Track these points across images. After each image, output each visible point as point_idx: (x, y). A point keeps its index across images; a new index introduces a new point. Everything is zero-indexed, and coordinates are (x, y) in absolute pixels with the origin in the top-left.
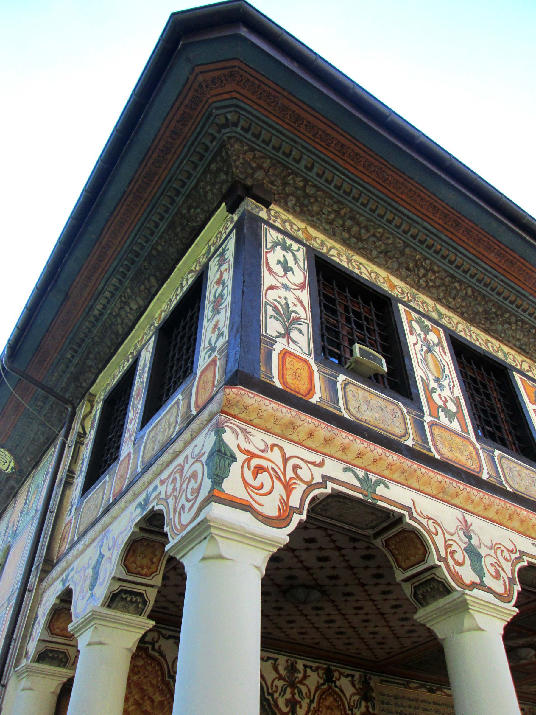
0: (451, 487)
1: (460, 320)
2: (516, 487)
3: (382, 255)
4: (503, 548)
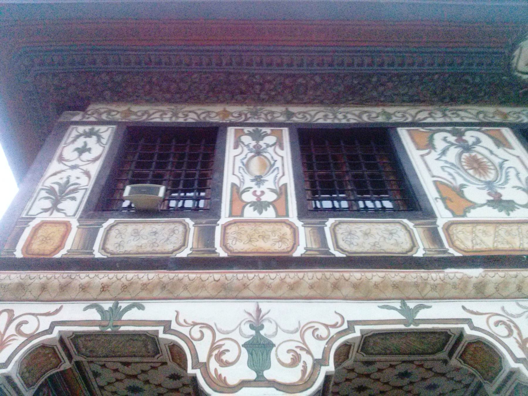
0: (235, 281)
1: (322, 108)
2: (354, 249)
3: (211, 94)
4: (317, 326)
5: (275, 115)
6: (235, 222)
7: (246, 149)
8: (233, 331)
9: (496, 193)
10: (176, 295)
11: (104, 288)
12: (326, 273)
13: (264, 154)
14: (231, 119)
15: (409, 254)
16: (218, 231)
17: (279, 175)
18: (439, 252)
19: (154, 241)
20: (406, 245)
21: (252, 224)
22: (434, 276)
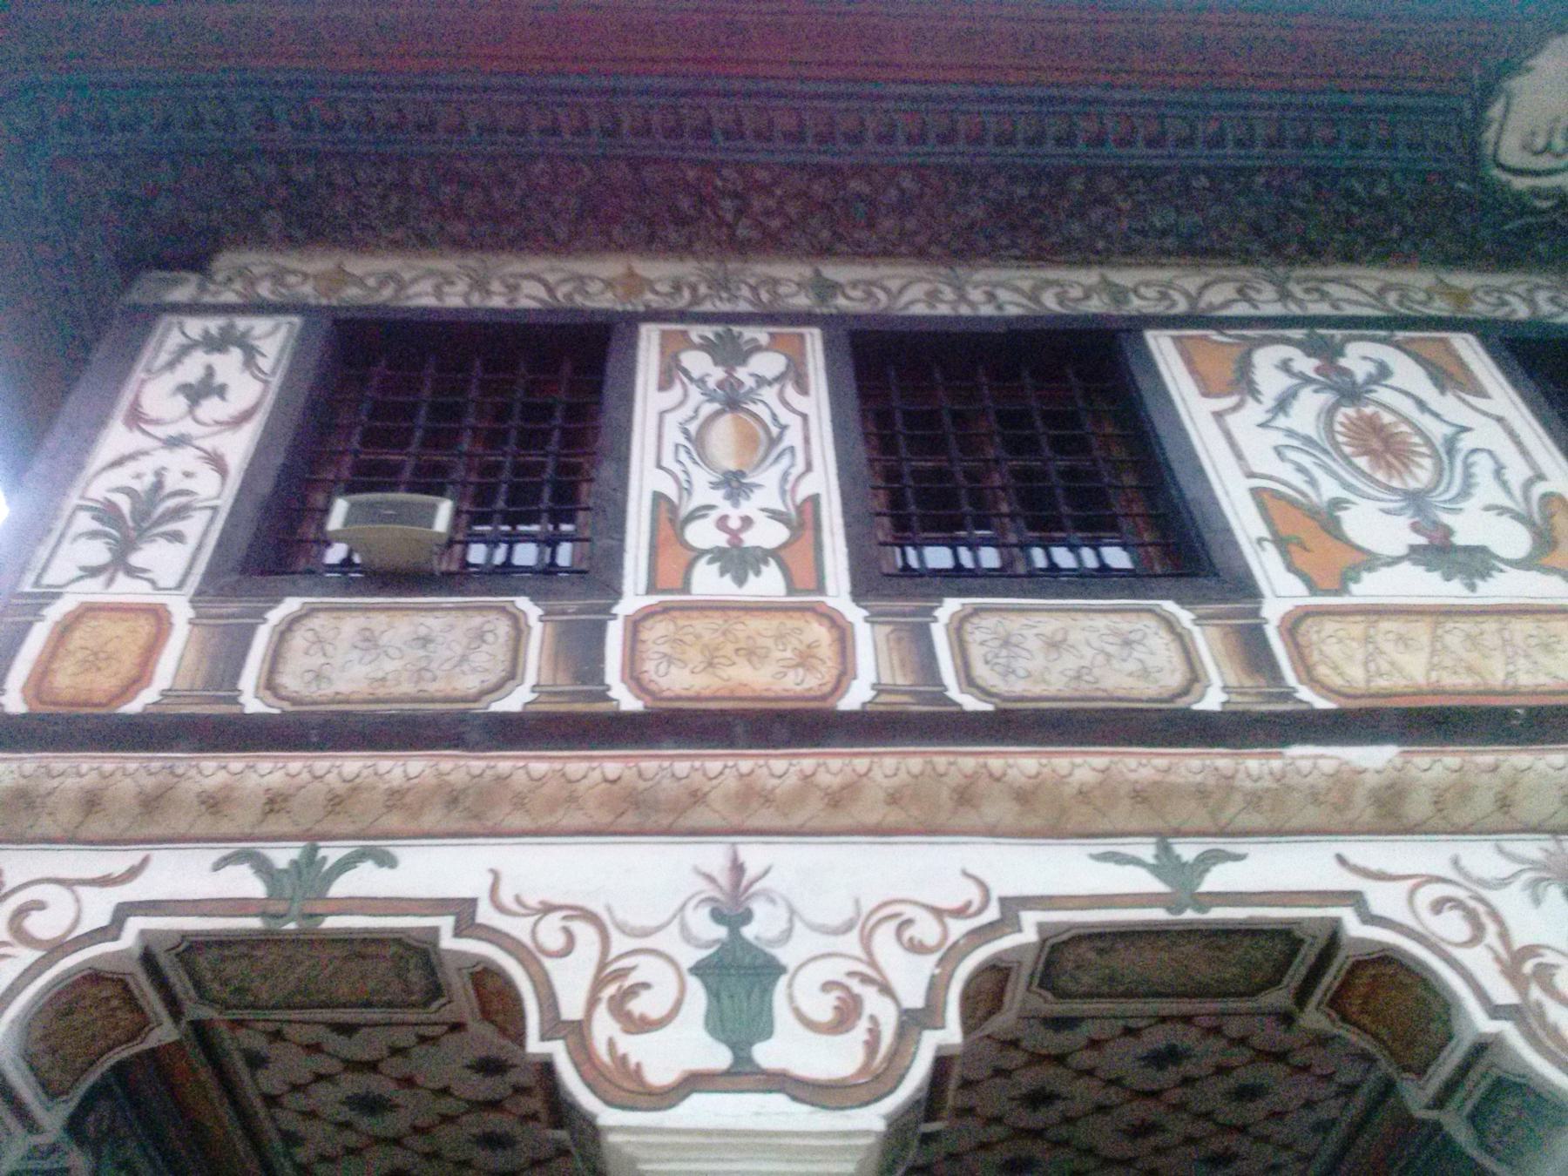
0: (666, 783)
1: (923, 271)
2: (1018, 687)
4: (909, 911)
5: (782, 290)
6: (666, 609)
7: (695, 392)
8: (659, 929)
9: (1436, 524)
10: (490, 824)
11: (275, 803)
12: (936, 759)
13: (752, 407)
14: (655, 301)
15: (1180, 703)
16: (615, 635)
17: (796, 471)
18: (1271, 697)
19: (423, 664)
20: (1171, 677)
21: (717, 614)
22: (1255, 766)
